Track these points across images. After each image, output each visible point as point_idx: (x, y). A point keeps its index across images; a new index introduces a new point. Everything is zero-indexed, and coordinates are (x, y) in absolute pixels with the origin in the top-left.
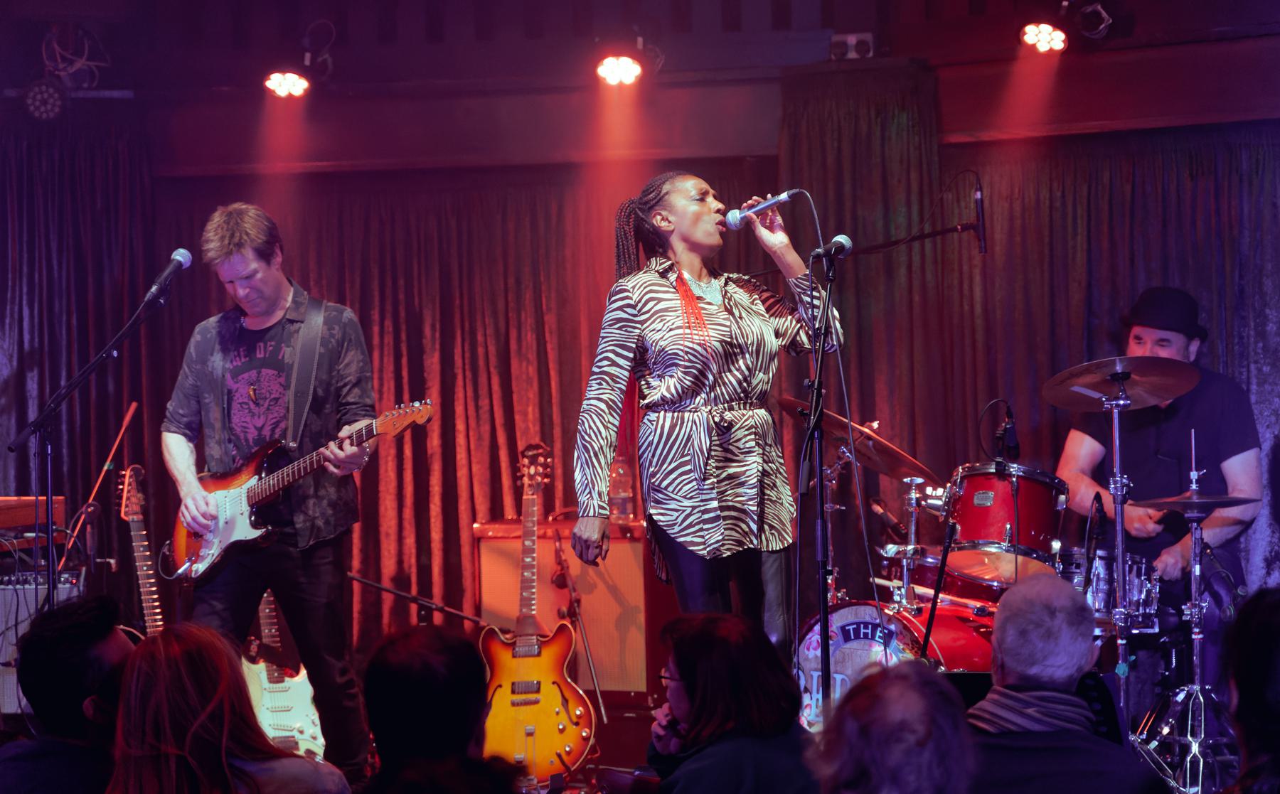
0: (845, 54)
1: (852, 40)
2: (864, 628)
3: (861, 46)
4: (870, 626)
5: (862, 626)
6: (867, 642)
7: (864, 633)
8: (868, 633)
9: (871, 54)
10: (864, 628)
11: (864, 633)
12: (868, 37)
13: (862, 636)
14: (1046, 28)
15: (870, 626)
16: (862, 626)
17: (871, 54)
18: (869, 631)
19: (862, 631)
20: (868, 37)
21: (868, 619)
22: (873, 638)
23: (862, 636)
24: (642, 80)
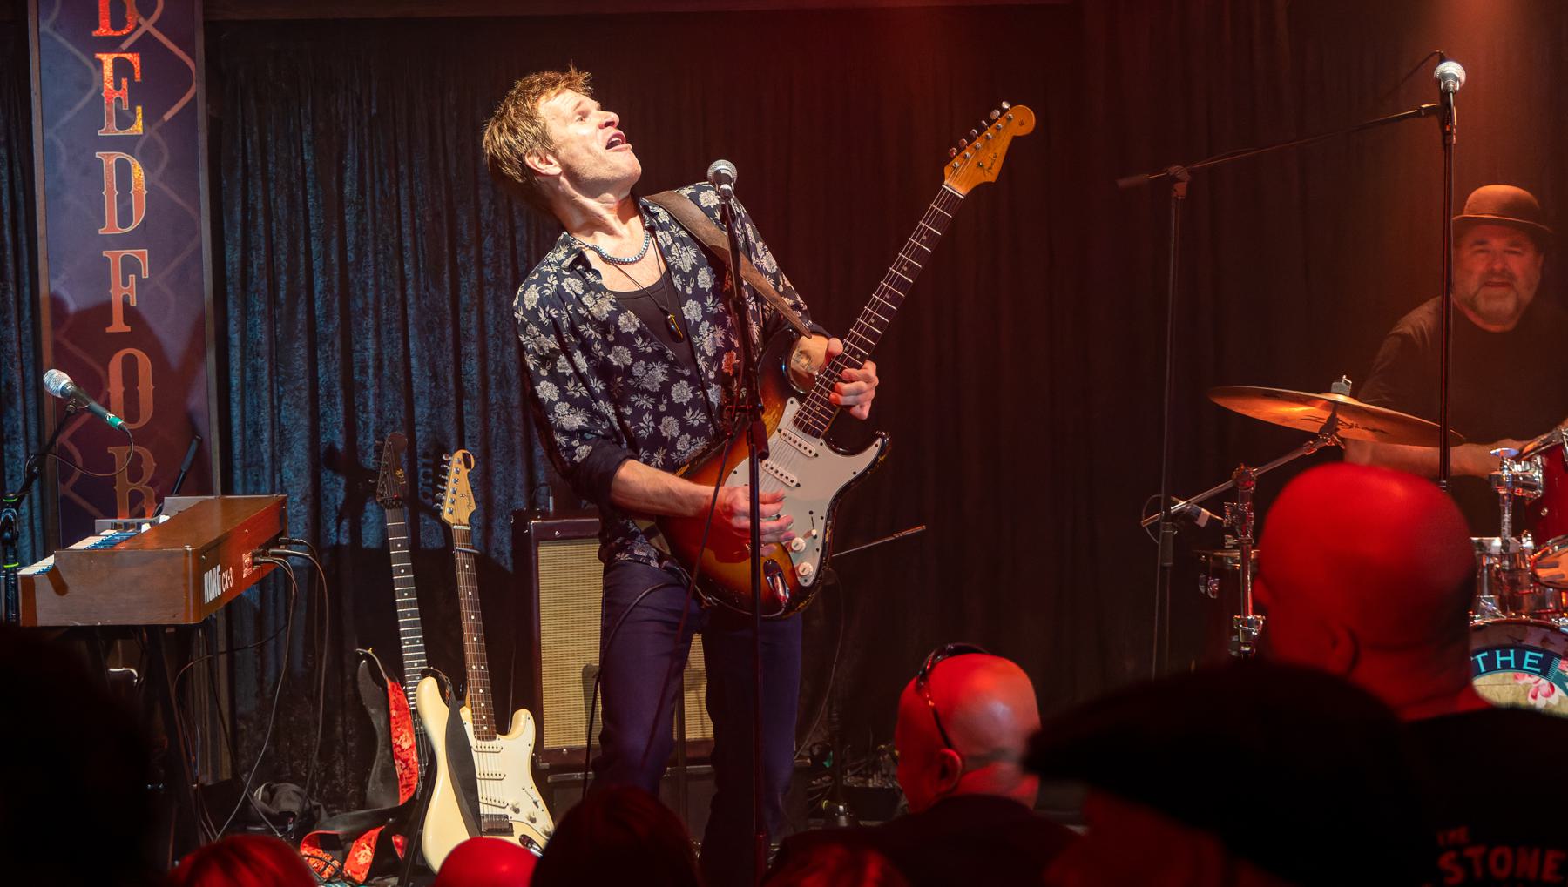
2: (1501, 656)
4: (1512, 652)
5: (1498, 652)
6: (1510, 674)
7: (1501, 661)
8: (1510, 660)
10: (1501, 656)
11: (1501, 661)
13: (1499, 666)
15: (1512, 652)
16: (1498, 652)
18: (1512, 658)
19: (1499, 659)
21: (1509, 642)
22: (1519, 666)
23: (1499, 666)
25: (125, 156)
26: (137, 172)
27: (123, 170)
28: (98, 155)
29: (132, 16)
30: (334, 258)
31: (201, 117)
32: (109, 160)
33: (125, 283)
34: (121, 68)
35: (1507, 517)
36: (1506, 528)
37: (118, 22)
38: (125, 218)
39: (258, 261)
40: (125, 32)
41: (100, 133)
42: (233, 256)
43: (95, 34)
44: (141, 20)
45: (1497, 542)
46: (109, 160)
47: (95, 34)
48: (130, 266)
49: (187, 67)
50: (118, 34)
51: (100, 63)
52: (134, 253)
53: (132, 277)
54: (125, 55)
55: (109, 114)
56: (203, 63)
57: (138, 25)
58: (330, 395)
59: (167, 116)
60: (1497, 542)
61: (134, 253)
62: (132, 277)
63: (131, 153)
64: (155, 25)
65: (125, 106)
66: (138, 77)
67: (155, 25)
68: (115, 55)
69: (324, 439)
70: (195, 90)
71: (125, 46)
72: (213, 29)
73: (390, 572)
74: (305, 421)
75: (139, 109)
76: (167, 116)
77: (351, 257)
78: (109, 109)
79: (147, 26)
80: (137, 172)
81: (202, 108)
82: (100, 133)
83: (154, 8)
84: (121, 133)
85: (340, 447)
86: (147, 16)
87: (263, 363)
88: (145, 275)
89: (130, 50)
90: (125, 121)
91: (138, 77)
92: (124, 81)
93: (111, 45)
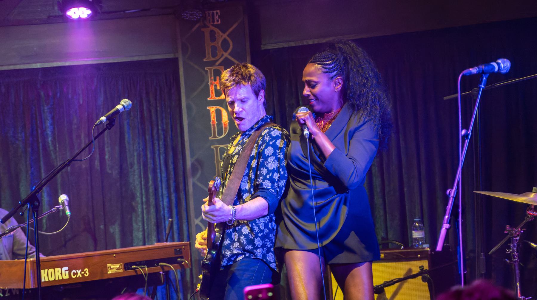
25: (218, 107)
27: (219, 114)
28: (208, 108)
29: (220, 52)
32: (212, 109)
37: (214, 55)
40: (216, 58)
41: (208, 99)
43: (205, 60)
44: (224, 53)
46: (212, 109)
50: (213, 59)
51: (207, 72)
52: (225, 146)
57: (223, 55)
61: (225, 146)
63: (222, 107)
64: (230, 54)
67: (230, 54)
71: (217, 63)
78: (212, 89)
79: (226, 55)
82: (208, 99)
84: (217, 98)
86: (226, 51)
89: (220, 65)
93: (213, 63)
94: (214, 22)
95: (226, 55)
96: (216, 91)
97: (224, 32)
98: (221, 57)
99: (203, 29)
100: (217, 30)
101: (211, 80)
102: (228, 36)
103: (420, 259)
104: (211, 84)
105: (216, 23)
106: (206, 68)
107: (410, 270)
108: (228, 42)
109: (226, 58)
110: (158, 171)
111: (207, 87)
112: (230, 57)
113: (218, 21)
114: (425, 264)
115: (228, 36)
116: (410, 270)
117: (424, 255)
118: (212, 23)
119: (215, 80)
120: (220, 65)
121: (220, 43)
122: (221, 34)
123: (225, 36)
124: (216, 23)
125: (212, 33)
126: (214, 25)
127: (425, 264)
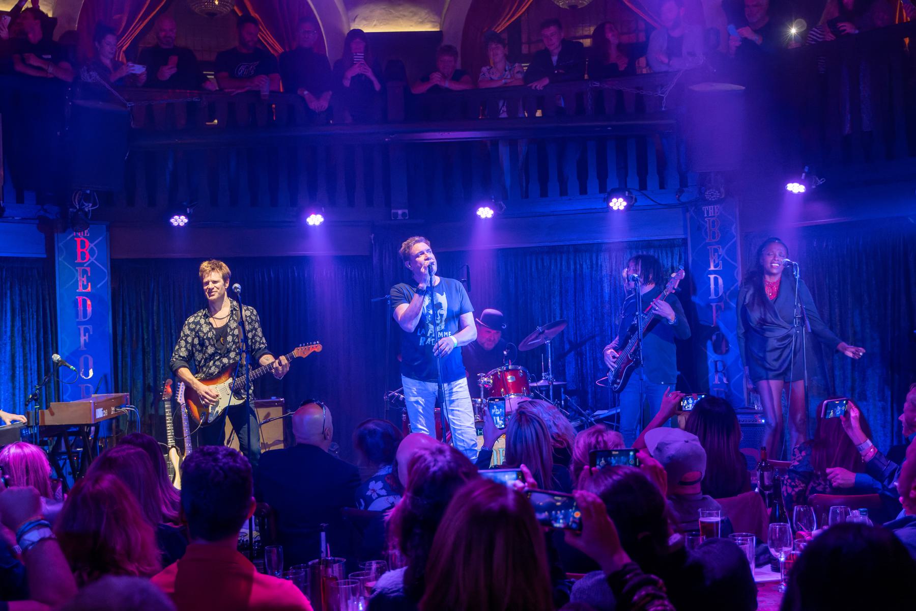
0: (397, 217)
1: (400, 212)
3: (404, 214)
9: (407, 218)
12: (407, 211)
14: (487, 209)
17: (407, 218)
20: (407, 211)
24: (322, 224)
25: (86, 298)
26: (89, 302)
27: (85, 302)
30: (150, 328)
31: (109, 286)
33: (85, 336)
34: (85, 272)
35: (482, 393)
36: (482, 396)
37: (83, 258)
38: (85, 315)
39: (127, 329)
40: (84, 262)
42: (120, 329)
43: (76, 262)
44: (91, 258)
45: (480, 400)
46: (80, 299)
47: (76, 262)
48: (86, 330)
49: (105, 272)
53: (87, 334)
54: (86, 268)
55: (80, 285)
56: (110, 271)
57: (90, 259)
58: (149, 369)
59: (99, 286)
60: (480, 400)
62: (87, 334)
64: (95, 259)
65: (85, 283)
66: (89, 275)
67: (95, 259)
68: (83, 268)
69: (147, 383)
70: (107, 278)
71: (85, 265)
72: (113, 261)
73: (165, 420)
74: (141, 377)
75: (89, 284)
76: (99, 286)
77: (155, 328)
78: (80, 284)
79: (92, 259)
80: (89, 302)
81: (109, 283)
83: (95, 254)
84: (83, 291)
85: (152, 384)
86: (92, 257)
87: (129, 360)
88: (91, 333)
90: (85, 287)
91: (89, 275)
92: (85, 276)
93: (81, 265)
94: (84, 234)
95: (92, 259)
96: (83, 285)
97: (92, 243)
98: (88, 261)
99: (75, 239)
100: (86, 241)
101: (80, 276)
102: (95, 245)
103: (278, 406)
104: (80, 280)
105: (86, 235)
106: (77, 268)
107: (268, 414)
108: (94, 250)
109: (92, 261)
110: (32, 343)
111: (77, 281)
112: (96, 262)
113: (87, 234)
114: (280, 409)
115: (95, 245)
116: (268, 414)
117: (280, 404)
118: (82, 235)
119: (83, 277)
120: (87, 267)
121: (88, 251)
122: (89, 244)
123: (92, 245)
124: (86, 235)
125: (83, 242)
126: (85, 237)
127: (280, 409)
